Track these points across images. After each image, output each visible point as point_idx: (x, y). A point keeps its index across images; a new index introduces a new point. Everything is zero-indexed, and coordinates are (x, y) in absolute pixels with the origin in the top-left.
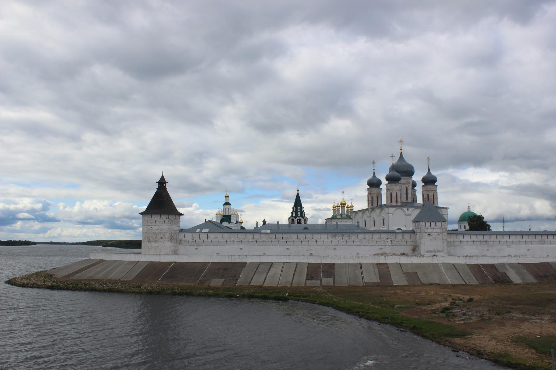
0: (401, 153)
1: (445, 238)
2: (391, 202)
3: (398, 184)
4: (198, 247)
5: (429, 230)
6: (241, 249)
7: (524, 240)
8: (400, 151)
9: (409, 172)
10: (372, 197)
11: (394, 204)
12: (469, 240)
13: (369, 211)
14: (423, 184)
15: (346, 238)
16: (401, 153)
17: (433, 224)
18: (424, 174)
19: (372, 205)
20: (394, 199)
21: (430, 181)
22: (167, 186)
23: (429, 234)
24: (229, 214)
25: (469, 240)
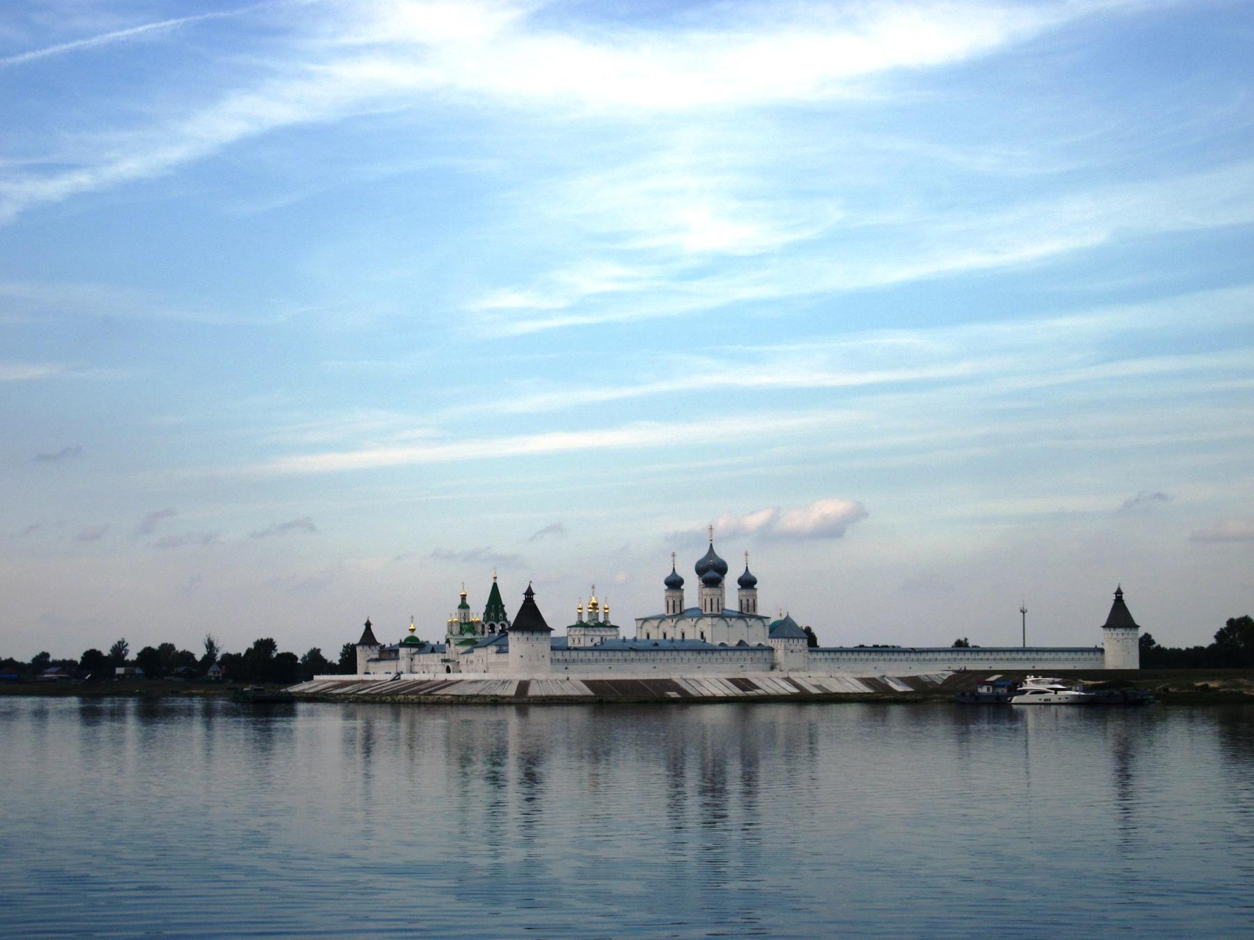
0: (711, 544)
1: (806, 655)
2: (712, 610)
3: (715, 589)
4: (568, 667)
5: (792, 647)
6: (610, 668)
7: (871, 657)
8: (710, 542)
9: (722, 569)
10: (674, 601)
11: (715, 612)
12: (823, 657)
13: (674, 621)
14: (740, 587)
15: (709, 655)
16: (711, 544)
17: (795, 640)
18: (740, 572)
19: (674, 612)
20: (715, 607)
21: (747, 583)
22: (535, 598)
23: (792, 651)
24: (695, 636)
25: (823, 657)
